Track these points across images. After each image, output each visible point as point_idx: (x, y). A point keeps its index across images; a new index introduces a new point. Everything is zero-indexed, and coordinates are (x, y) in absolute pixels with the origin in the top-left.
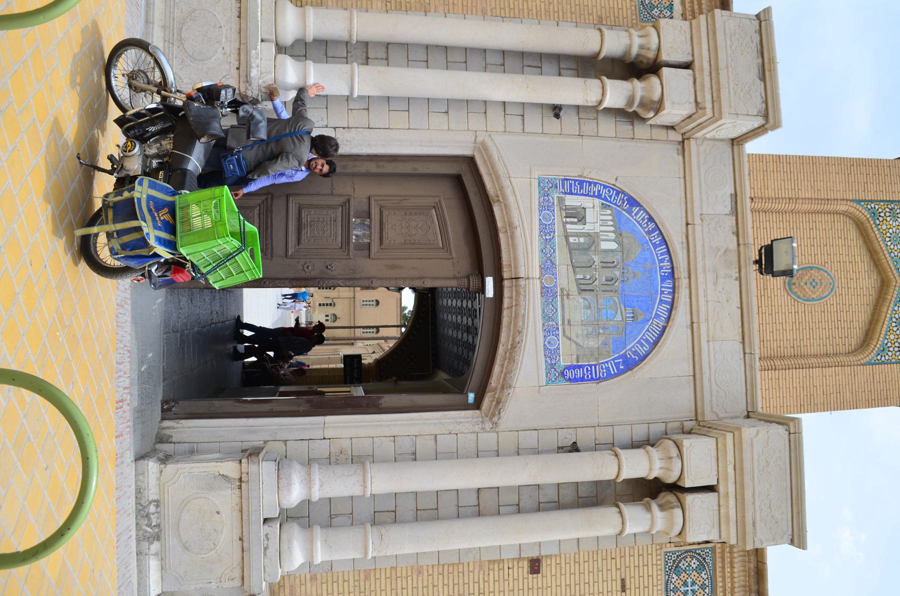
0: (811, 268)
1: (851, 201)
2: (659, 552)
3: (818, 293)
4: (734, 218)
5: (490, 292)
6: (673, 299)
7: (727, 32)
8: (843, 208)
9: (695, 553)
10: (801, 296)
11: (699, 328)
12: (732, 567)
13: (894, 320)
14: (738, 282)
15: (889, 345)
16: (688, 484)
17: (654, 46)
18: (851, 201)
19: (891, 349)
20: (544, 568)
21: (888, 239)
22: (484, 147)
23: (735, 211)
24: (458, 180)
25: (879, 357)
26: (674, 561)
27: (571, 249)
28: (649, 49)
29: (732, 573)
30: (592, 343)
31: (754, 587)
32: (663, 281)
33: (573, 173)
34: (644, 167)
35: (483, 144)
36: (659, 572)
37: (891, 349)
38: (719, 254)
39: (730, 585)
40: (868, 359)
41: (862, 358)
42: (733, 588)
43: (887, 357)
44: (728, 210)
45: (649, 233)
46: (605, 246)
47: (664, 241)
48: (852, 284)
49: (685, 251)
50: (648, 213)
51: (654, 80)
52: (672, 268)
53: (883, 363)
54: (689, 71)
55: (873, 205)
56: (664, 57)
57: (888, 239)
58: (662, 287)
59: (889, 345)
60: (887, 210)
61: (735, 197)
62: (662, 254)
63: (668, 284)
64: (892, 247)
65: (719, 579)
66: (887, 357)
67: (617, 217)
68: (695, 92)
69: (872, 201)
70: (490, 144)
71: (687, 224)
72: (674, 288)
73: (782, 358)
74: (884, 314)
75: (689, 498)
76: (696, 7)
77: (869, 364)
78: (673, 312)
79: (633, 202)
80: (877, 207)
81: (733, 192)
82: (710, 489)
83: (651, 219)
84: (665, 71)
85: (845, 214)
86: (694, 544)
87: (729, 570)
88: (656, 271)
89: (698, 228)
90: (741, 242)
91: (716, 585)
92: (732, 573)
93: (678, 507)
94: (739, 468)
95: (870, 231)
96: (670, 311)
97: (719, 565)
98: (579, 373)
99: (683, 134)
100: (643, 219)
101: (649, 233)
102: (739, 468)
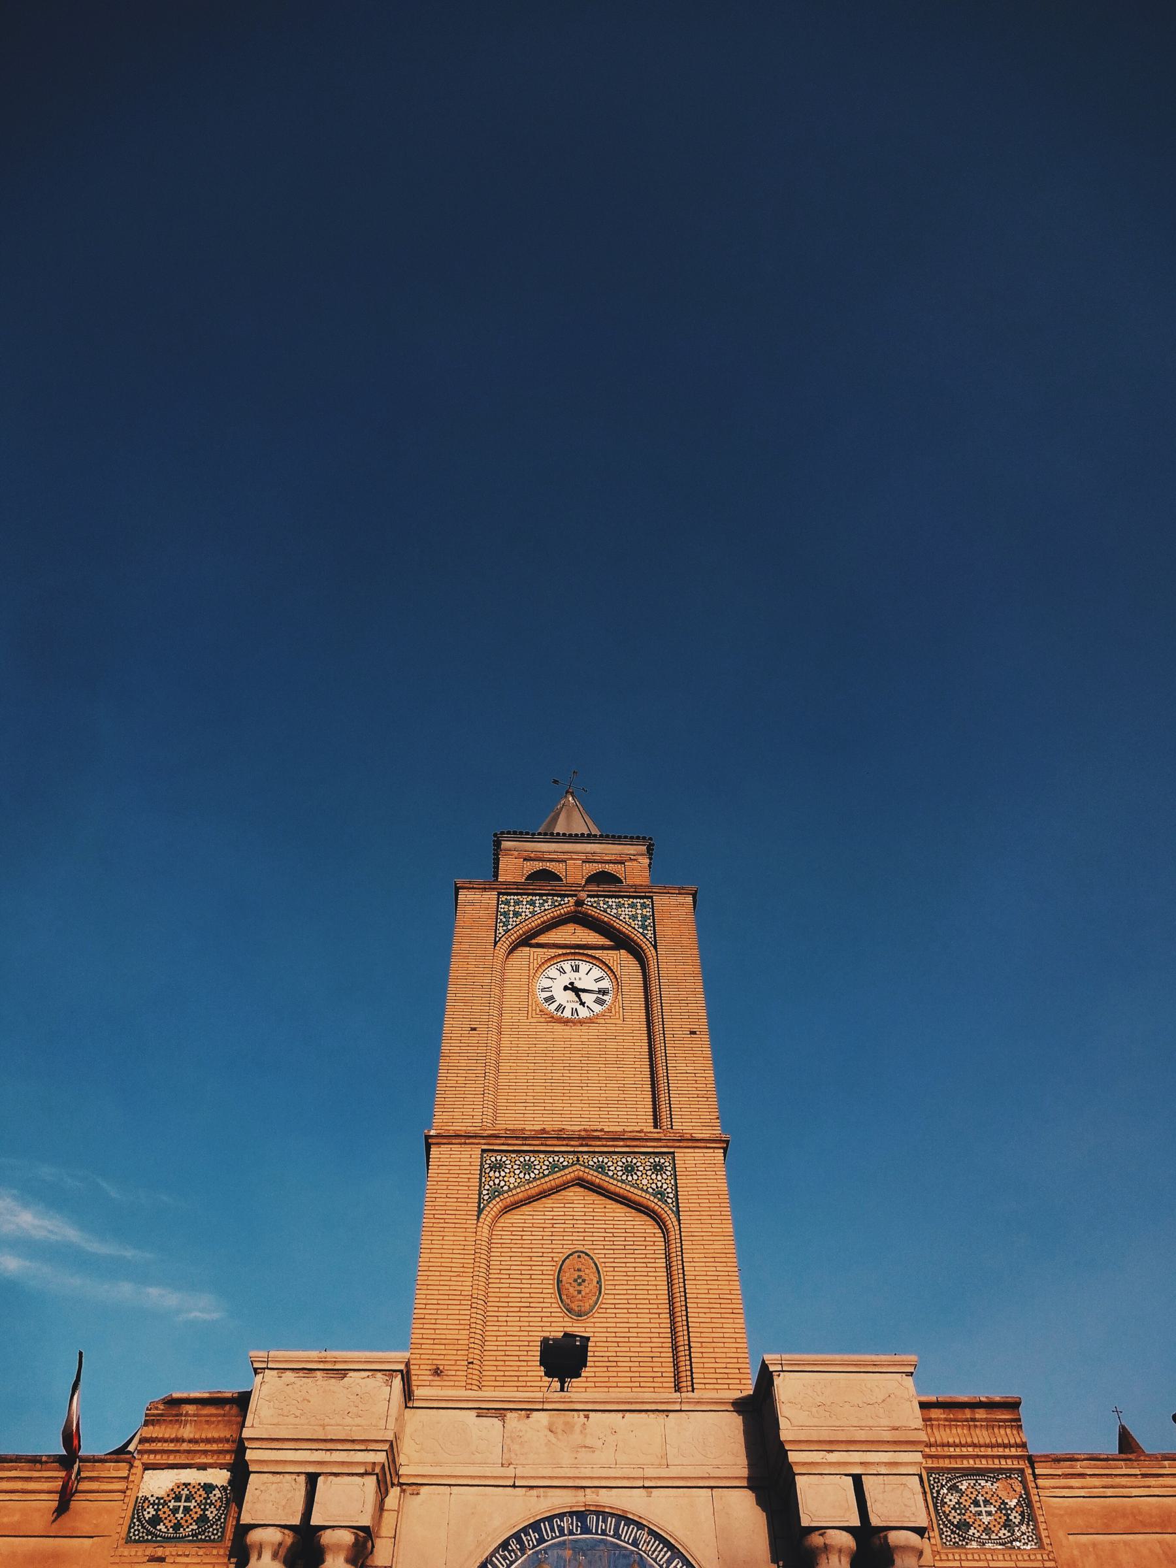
0: (559, 1281)
1: (478, 1219)
2: (944, 1557)
3: (592, 1276)
4: (509, 1415)
6: (613, 1515)
7: (275, 1421)
8: (486, 1230)
9: (937, 1498)
10: (594, 1298)
11: (650, 1479)
12: (949, 1445)
13: (624, 1177)
14: (591, 1414)
15: (654, 1186)
16: (856, 1522)
18: (478, 1219)
19: (659, 1184)
21: (527, 1177)
23: (500, 1413)
25: (670, 1201)
26: (953, 1532)
28: (280, 1544)
29: (955, 1445)
31: (968, 1414)
32: (589, 1532)
36: (970, 1557)
37: (659, 1184)
38: (554, 1440)
39: (970, 1449)
40: (672, 1216)
41: (671, 1222)
42: (974, 1445)
43: (669, 1190)
44: (497, 1422)
45: (523, 1550)
47: (535, 1526)
48: (580, 1225)
49: (551, 1492)
50: (496, 1550)
51: (327, 1537)
52: (571, 1514)
53: (676, 1196)
54: (321, 1479)
55: (485, 1192)
56: (296, 1521)
57: (527, 1177)
58: (596, 1533)
59: (654, 1186)
60: (492, 1174)
61: (482, 1412)
62: (553, 1530)
63: (592, 1520)
64: (536, 1172)
65: (965, 1464)
66: (669, 1190)
68: (349, 1474)
69: (480, 1194)
71: (514, 1486)
72: (597, 1513)
73: (674, 1332)
74: (618, 1190)
75: (875, 1521)
76: (215, 1447)
77: (678, 1213)
78: (630, 1516)
80: (487, 1187)
81: (474, 1413)
83: (505, 1545)
84: (315, 1521)
85: (491, 1228)
86: (926, 1500)
87: (952, 1449)
88: (576, 1541)
90: (540, 1407)
91: (973, 1469)
92: (955, 1445)
93: (886, 1537)
94: (830, 1445)
95: (516, 1198)
96: (629, 1522)
97: (946, 1463)
99: (393, 1485)
100: (505, 1558)
101: (523, 1550)
102: (830, 1445)
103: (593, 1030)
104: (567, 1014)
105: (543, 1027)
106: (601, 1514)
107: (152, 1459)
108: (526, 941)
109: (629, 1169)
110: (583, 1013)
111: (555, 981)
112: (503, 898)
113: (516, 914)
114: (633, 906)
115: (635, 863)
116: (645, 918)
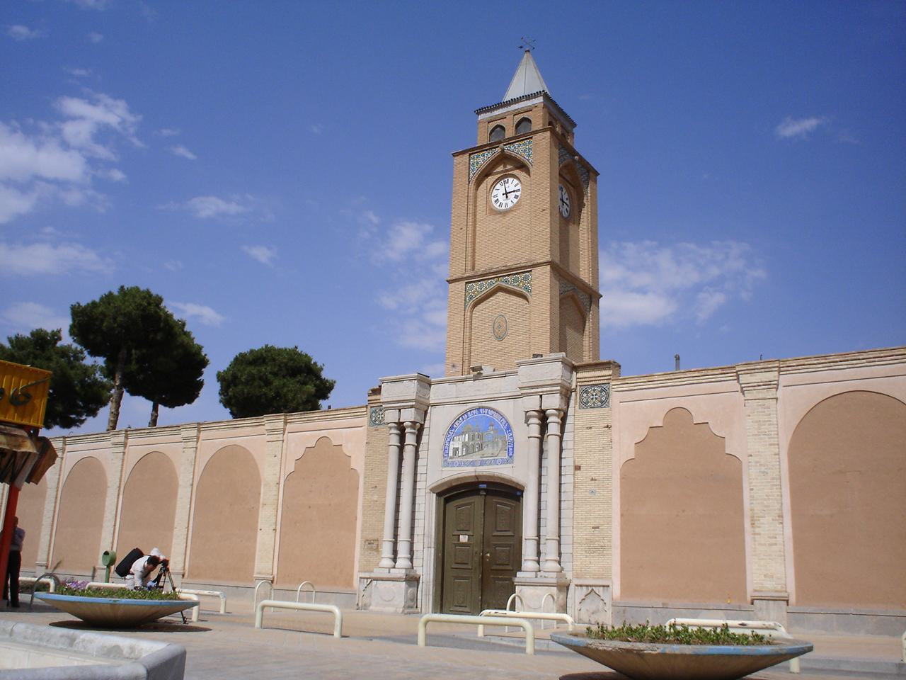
5: (484, 486)
17: (394, 425)
20: (577, 464)
22: (432, 490)
24: (447, 501)
27: (467, 454)
30: (500, 444)
33: (442, 452)
34: (438, 421)
35: (431, 490)
41: (530, 299)
46: (467, 440)
67: (458, 434)
70: (430, 488)
79: (452, 428)
82: (541, 396)
83: (458, 419)
89: (461, 399)
98: (511, 449)
103: (511, 215)
104: (503, 207)
105: (492, 217)
106: (483, 407)
107: (372, 405)
108: (486, 173)
109: (516, 281)
110: (510, 205)
111: (500, 189)
112: (472, 156)
113: (477, 163)
114: (525, 144)
115: (537, 109)
116: (530, 149)
